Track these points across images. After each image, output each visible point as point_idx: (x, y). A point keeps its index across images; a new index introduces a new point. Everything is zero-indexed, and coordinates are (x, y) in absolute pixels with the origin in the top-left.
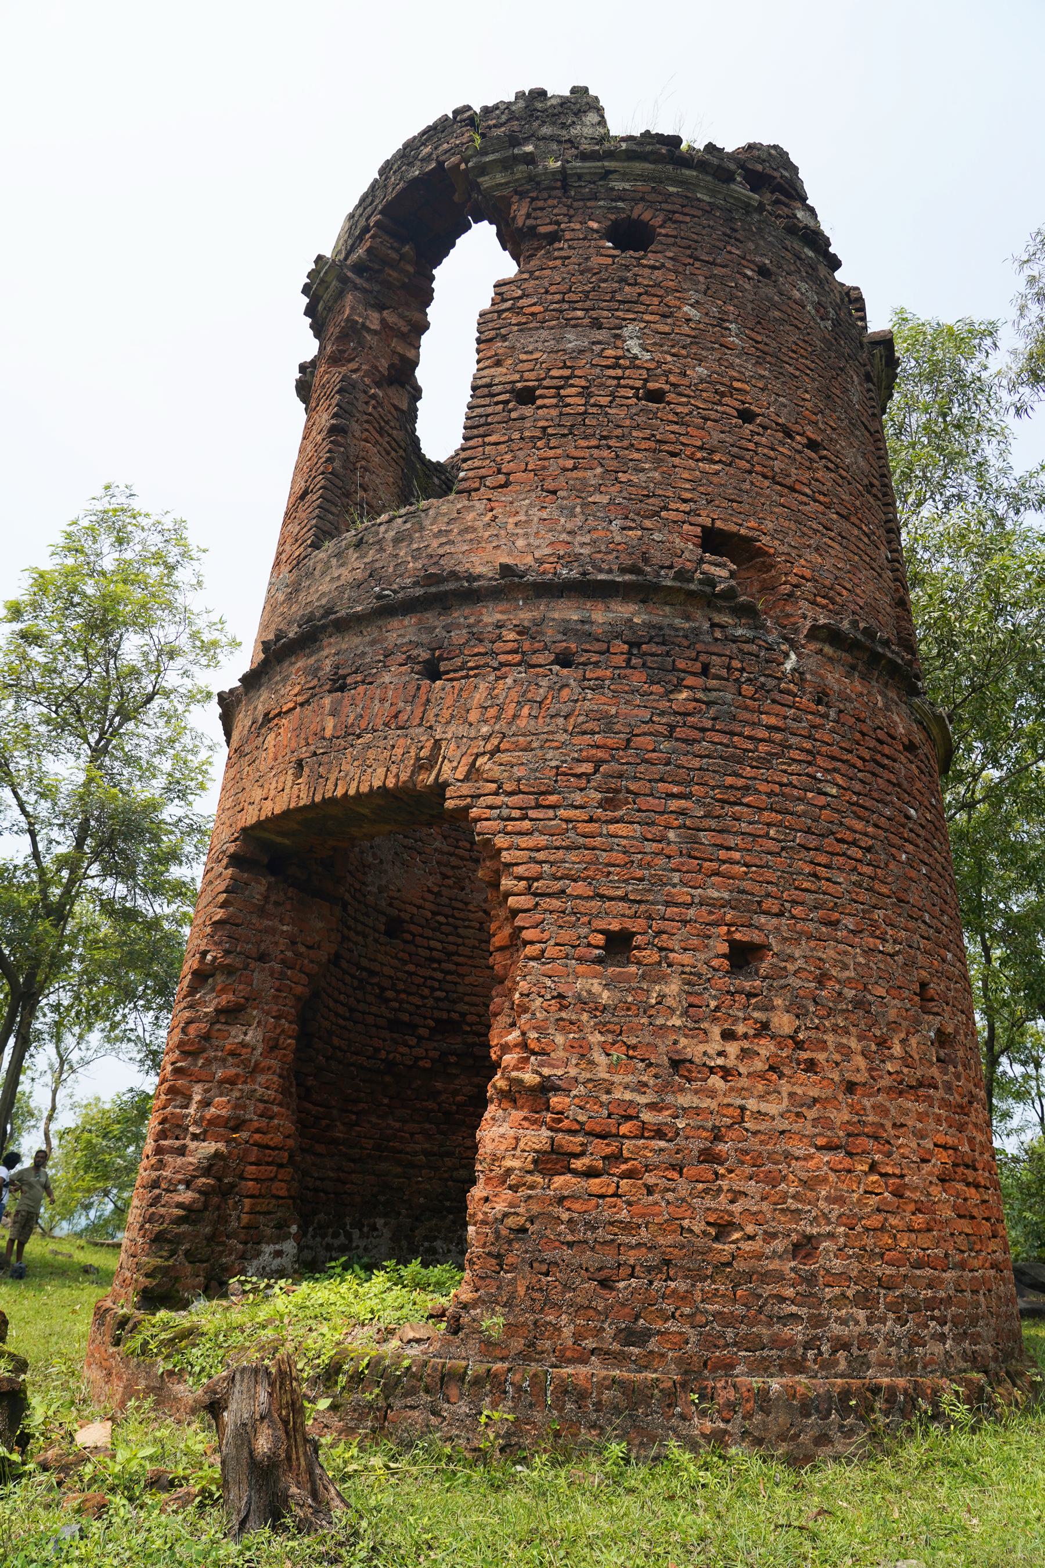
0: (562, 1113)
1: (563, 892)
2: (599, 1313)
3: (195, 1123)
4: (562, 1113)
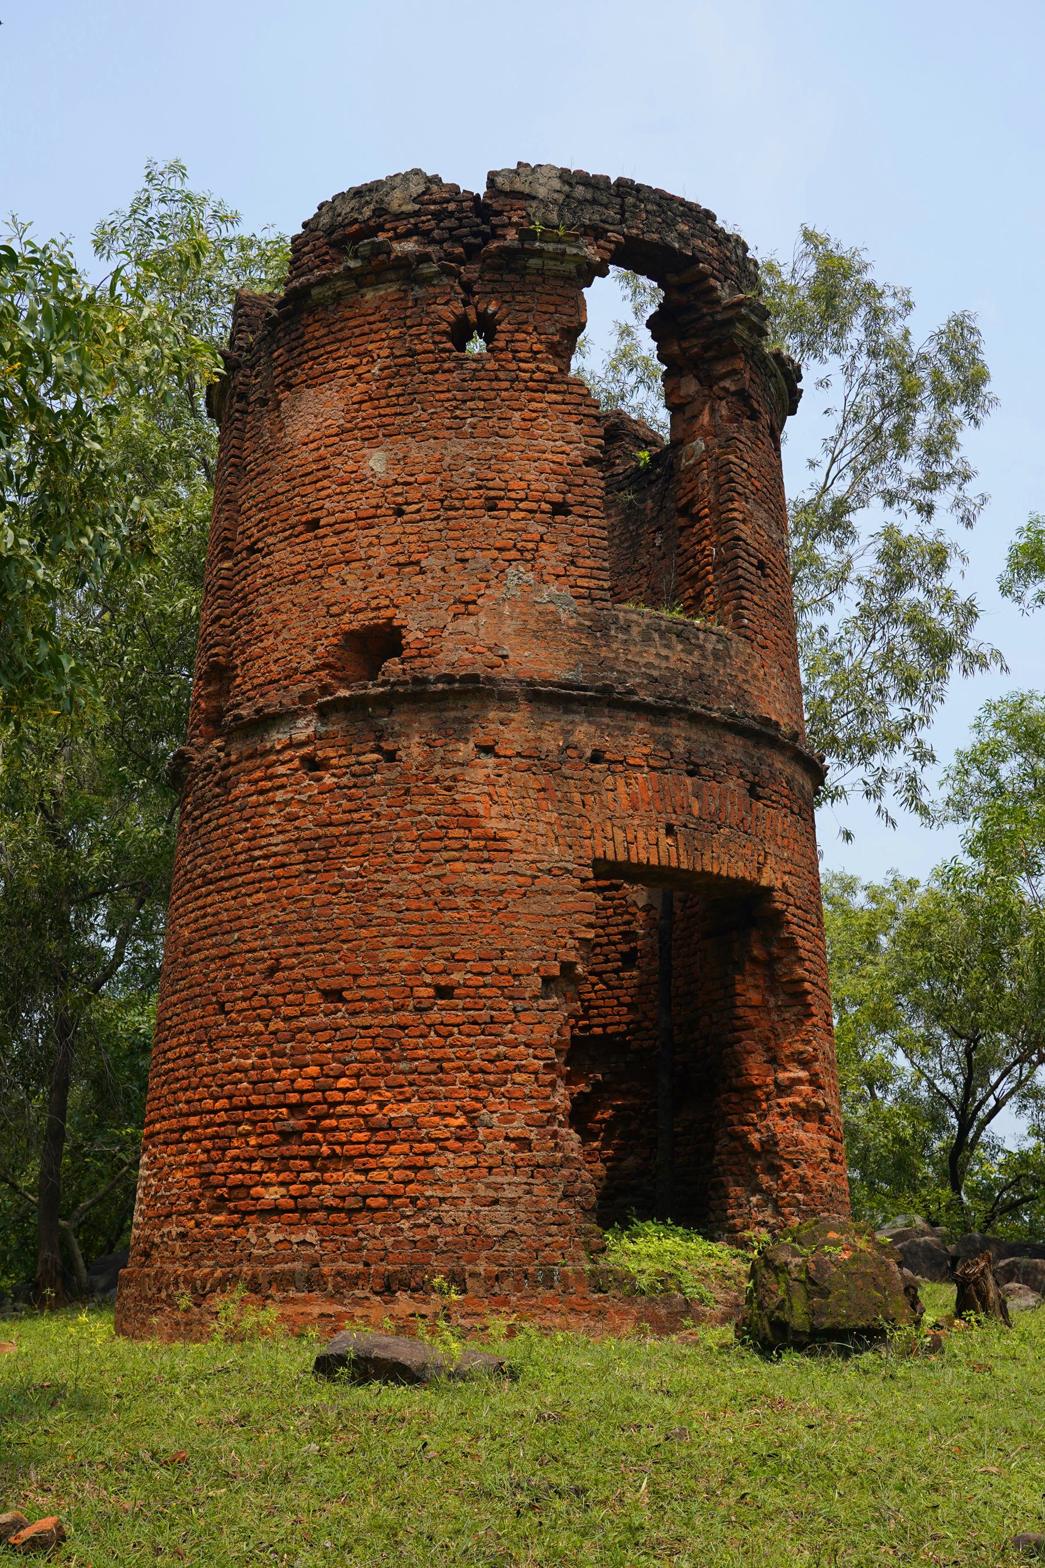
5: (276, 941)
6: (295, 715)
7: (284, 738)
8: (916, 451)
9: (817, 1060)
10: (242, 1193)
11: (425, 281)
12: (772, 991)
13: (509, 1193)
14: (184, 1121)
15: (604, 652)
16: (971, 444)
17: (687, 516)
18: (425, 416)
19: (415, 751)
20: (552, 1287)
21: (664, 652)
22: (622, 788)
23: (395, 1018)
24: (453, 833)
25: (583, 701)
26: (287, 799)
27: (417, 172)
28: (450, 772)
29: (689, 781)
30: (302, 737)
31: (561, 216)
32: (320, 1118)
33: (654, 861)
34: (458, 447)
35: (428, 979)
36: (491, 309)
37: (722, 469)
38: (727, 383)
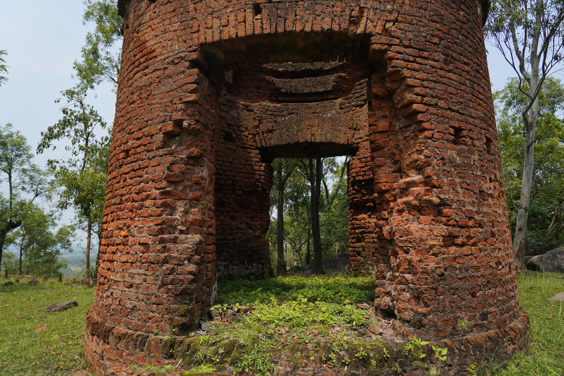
0: (449, 217)
1: (437, 104)
2: (474, 308)
3: (182, 224)
4: (449, 217)
9: (429, 165)
12: (395, 117)
20: (142, 350)
33: (241, 34)
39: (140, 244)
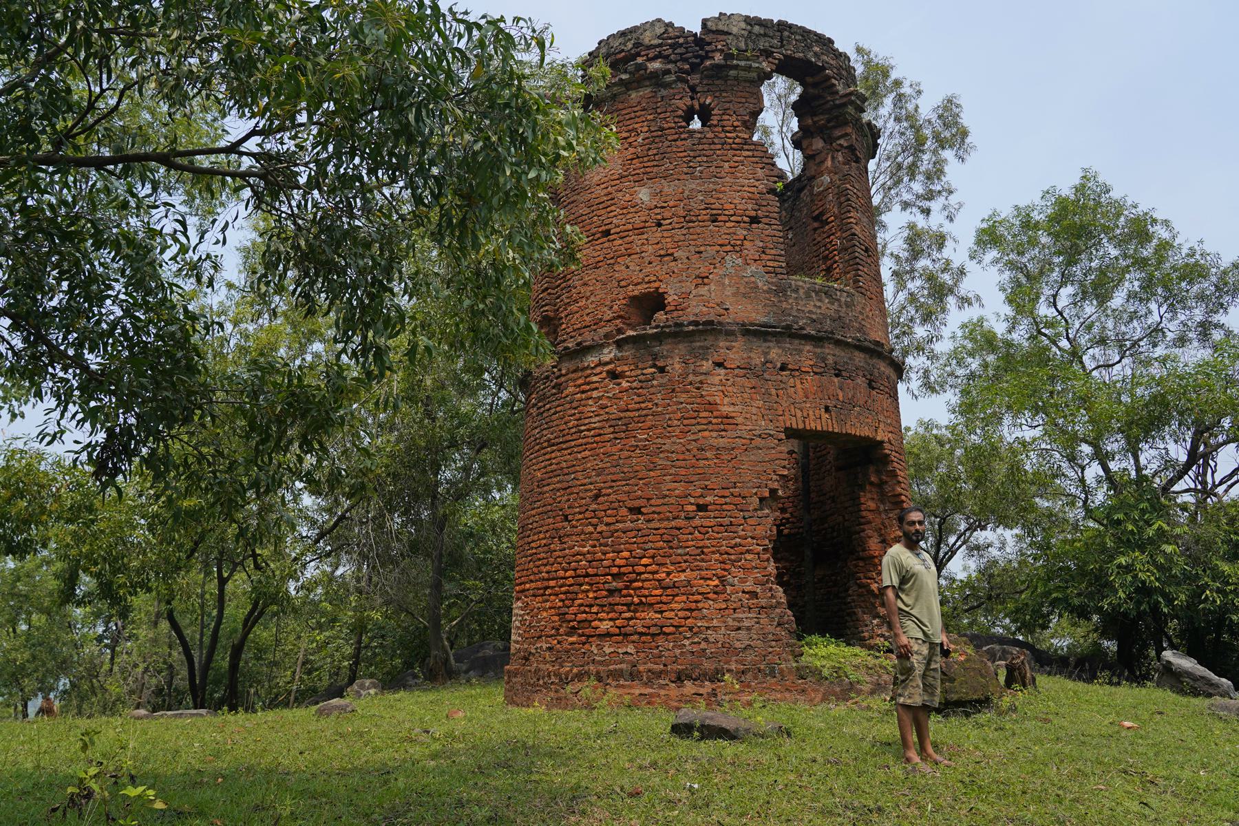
5: (598, 479)
6: (602, 346)
7: (596, 360)
8: (920, 177)
10: (586, 624)
11: (667, 86)
12: (882, 502)
13: (746, 624)
14: (546, 583)
15: (784, 305)
16: (954, 171)
17: (821, 225)
18: (672, 167)
19: (677, 366)
21: (818, 304)
22: (799, 386)
23: (673, 523)
24: (702, 415)
25: (774, 334)
26: (599, 396)
27: (659, 20)
28: (699, 379)
29: (836, 380)
30: (607, 359)
31: (746, 45)
32: (631, 582)
33: (819, 428)
34: (693, 185)
35: (692, 500)
36: (708, 102)
37: (842, 193)
38: (842, 142)
39: (744, 592)
